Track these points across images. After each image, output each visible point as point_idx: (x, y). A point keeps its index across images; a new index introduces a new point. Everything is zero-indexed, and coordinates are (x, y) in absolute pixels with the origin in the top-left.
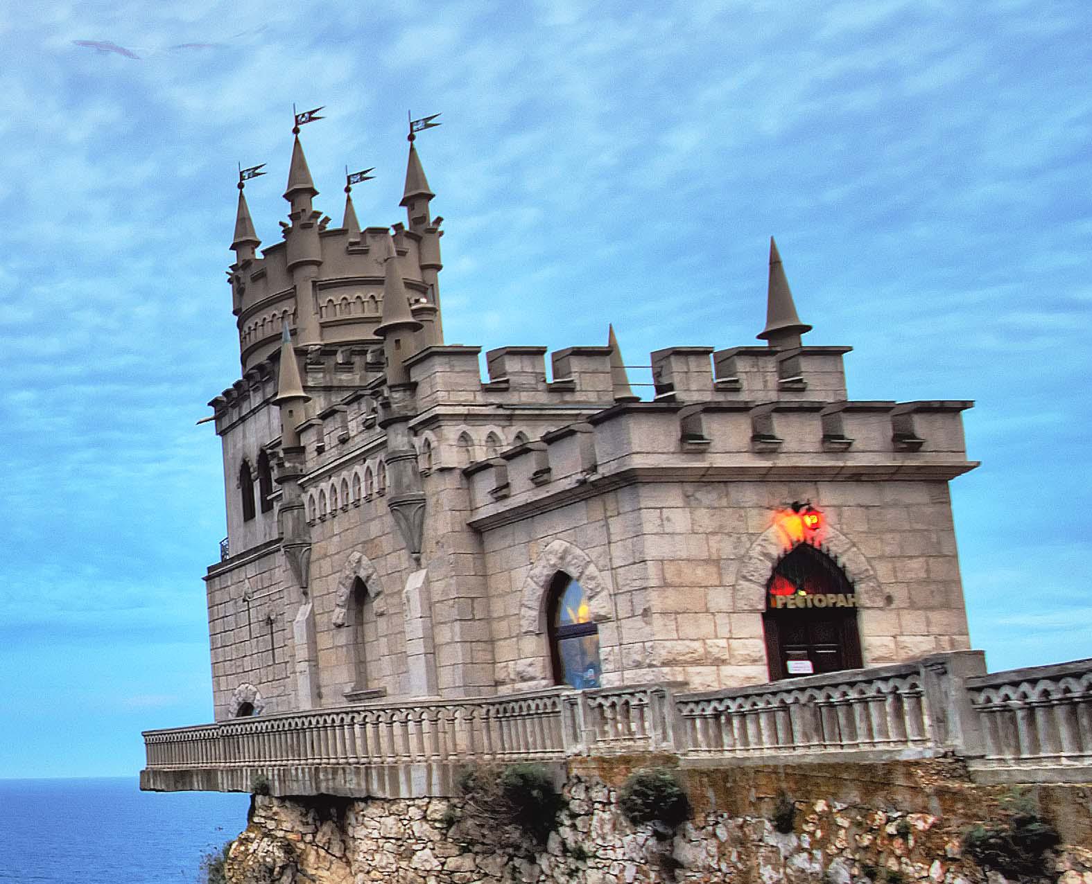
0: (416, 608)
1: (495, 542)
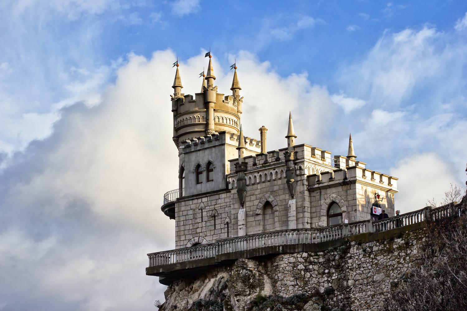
0: (293, 208)
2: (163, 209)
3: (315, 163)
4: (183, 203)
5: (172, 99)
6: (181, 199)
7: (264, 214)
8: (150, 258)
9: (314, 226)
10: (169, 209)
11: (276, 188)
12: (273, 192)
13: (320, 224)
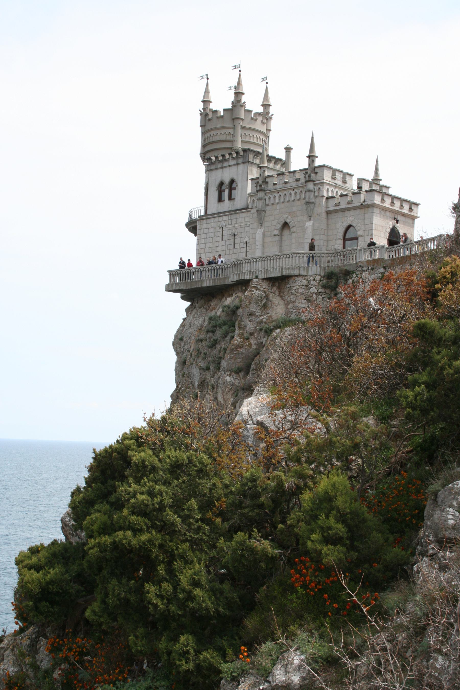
0: (310, 230)
1: (333, 217)
2: (187, 225)
3: (336, 186)
4: (205, 221)
5: (201, 114)
6: (206, 216)
7: (281, 234)
8: (170, 275)
9: (329, 249)
10: (192, 226)
11: (294, 209)
12: (291, 213)
13: (336, 247)
